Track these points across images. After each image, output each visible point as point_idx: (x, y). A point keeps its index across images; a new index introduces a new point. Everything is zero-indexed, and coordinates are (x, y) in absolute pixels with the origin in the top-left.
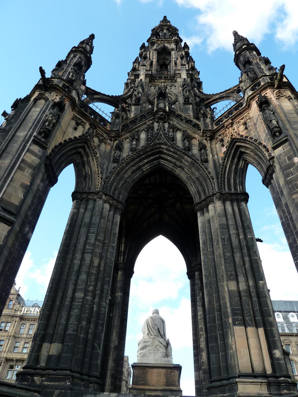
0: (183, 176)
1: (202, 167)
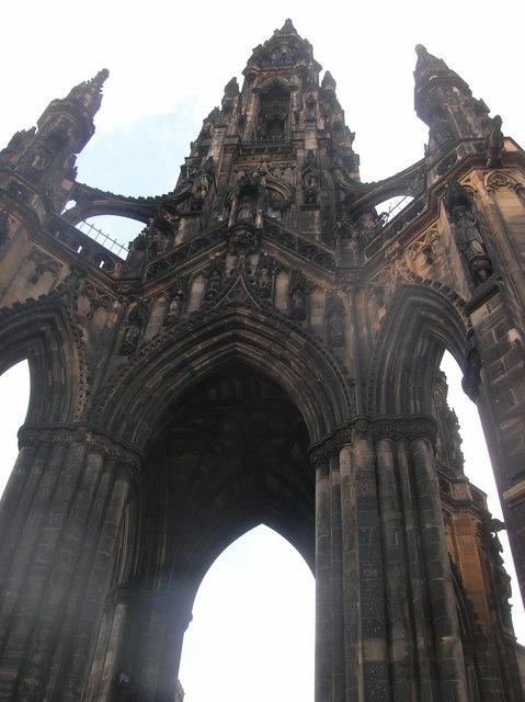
0: (287, 378)
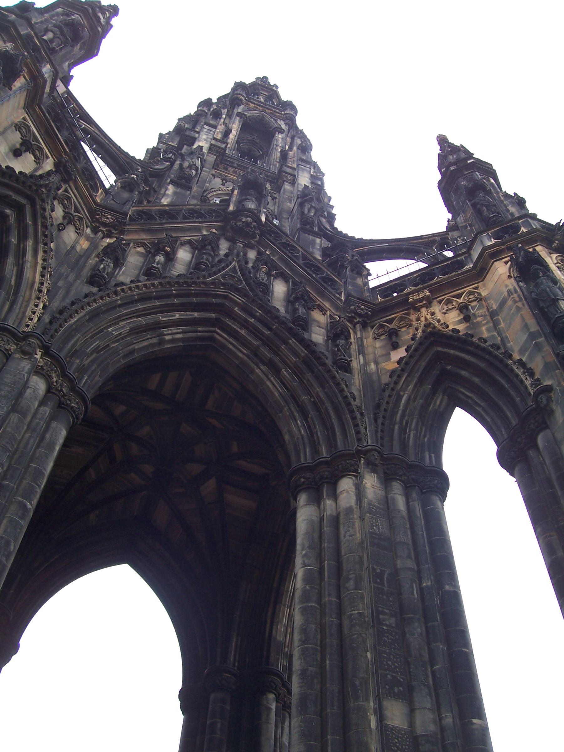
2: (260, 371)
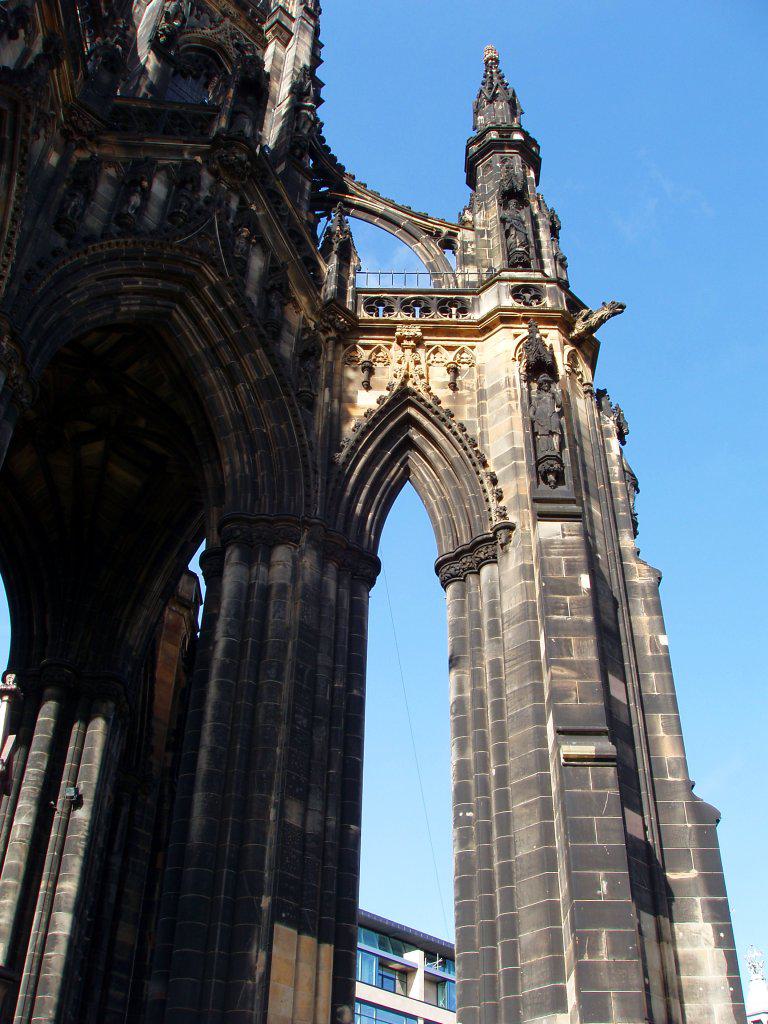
0: (223, 401)
1: (295, 416)
2: (212, 377)
